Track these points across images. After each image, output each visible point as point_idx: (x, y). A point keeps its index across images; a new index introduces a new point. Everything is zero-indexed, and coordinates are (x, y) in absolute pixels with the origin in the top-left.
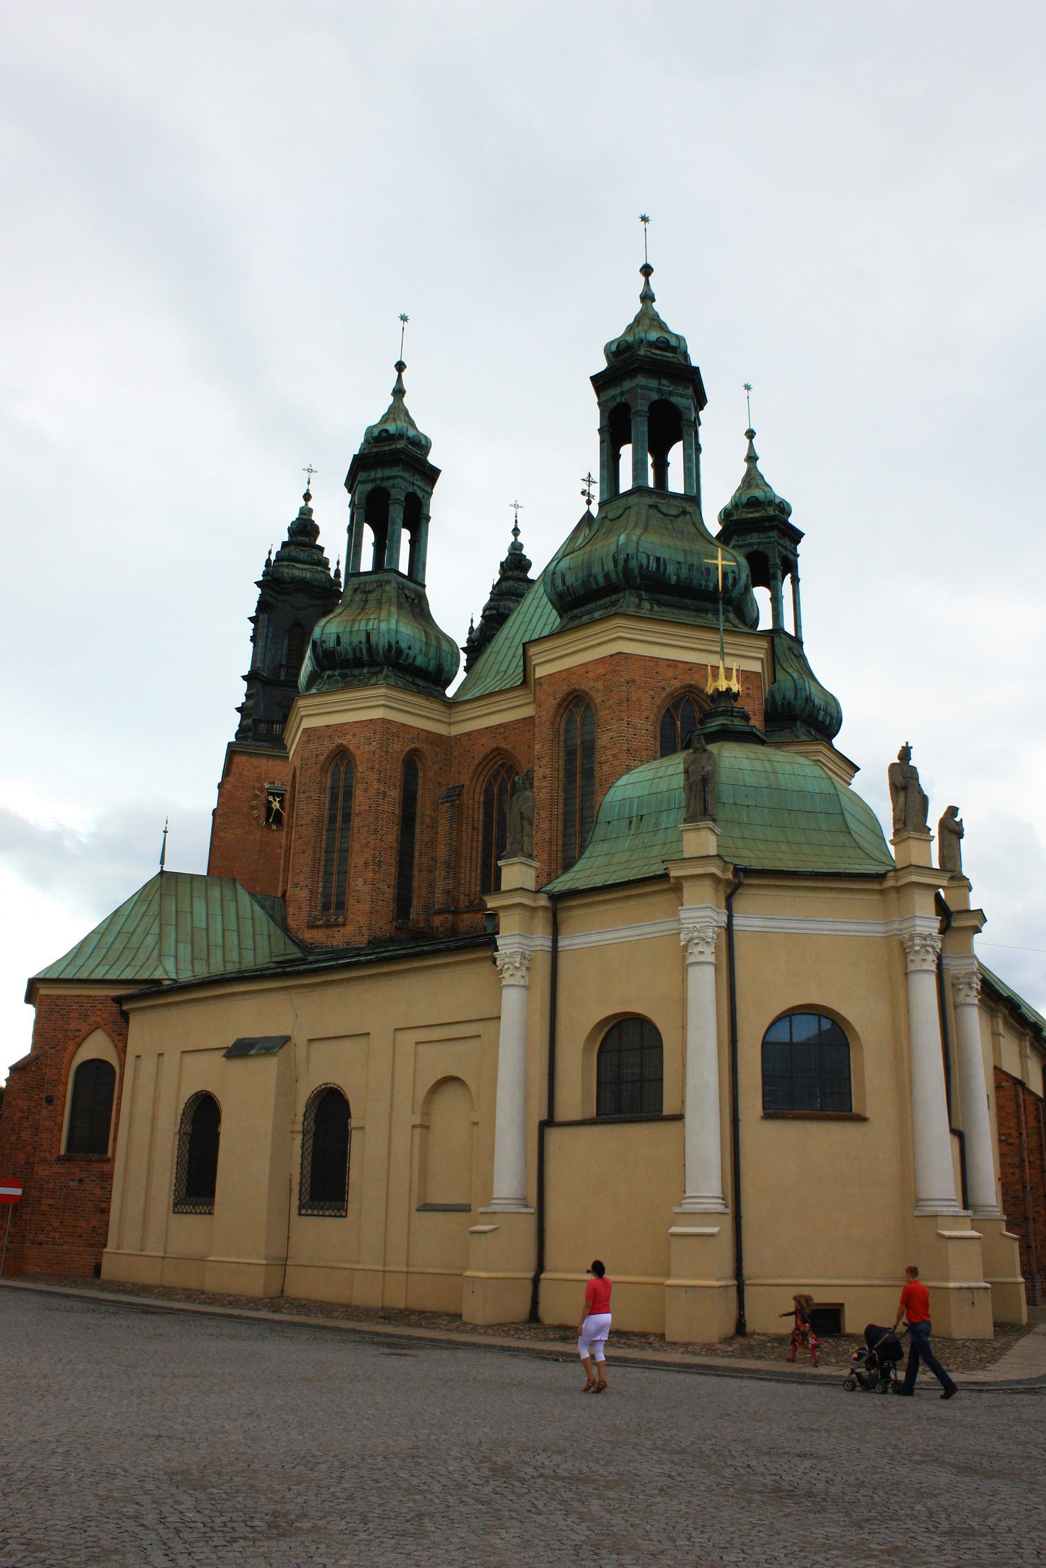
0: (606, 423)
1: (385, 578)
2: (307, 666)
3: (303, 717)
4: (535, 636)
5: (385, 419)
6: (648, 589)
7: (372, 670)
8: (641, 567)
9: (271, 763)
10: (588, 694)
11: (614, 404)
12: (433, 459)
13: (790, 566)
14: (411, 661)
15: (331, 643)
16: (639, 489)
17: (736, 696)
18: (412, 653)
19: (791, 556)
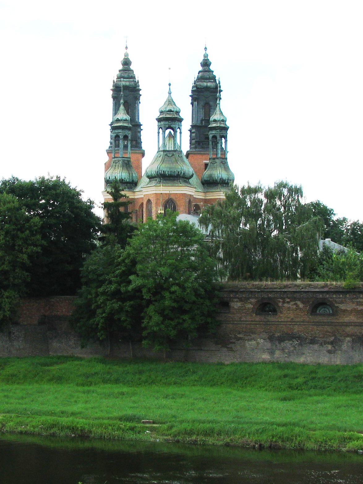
6: (162, 177)
15: (108, 178)
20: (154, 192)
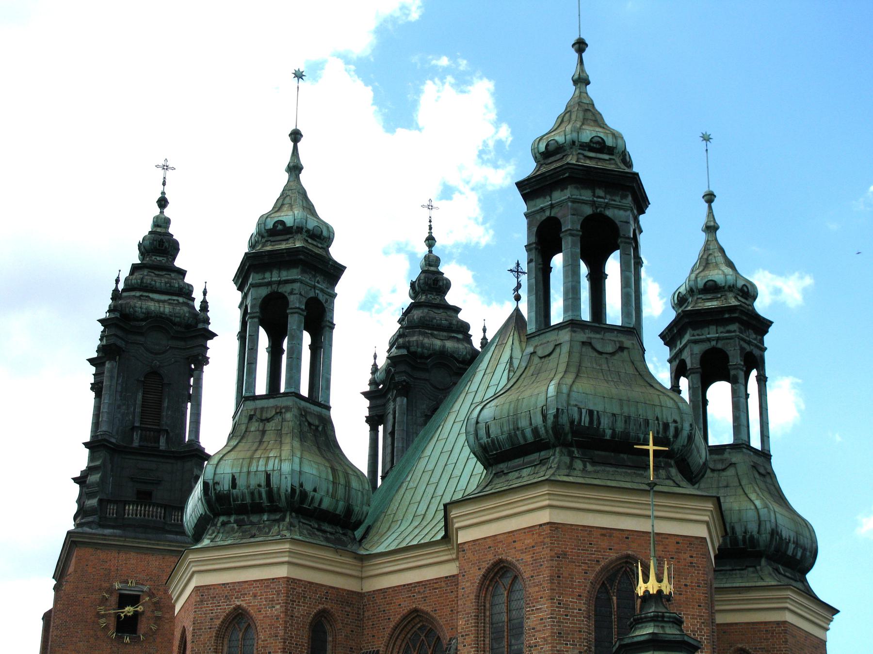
0: (533, 239)
1: (284, 404)
2: (194, 504)
3: (194, 573)
4: (458, 496)
5: (279, 206)
6: (579, 445)
7: (273, 517)
8: (572, 422)
9: (123, 556)
10: (515, 567)
11: (544, 218)
12: (337, 252)
13: (755, 360)
14: (316, 505)
15: (226, 485)
16: (573, 324)
17: (669, 598)
18: (318, 496)
19: (756, 352)
20: (544, 517)
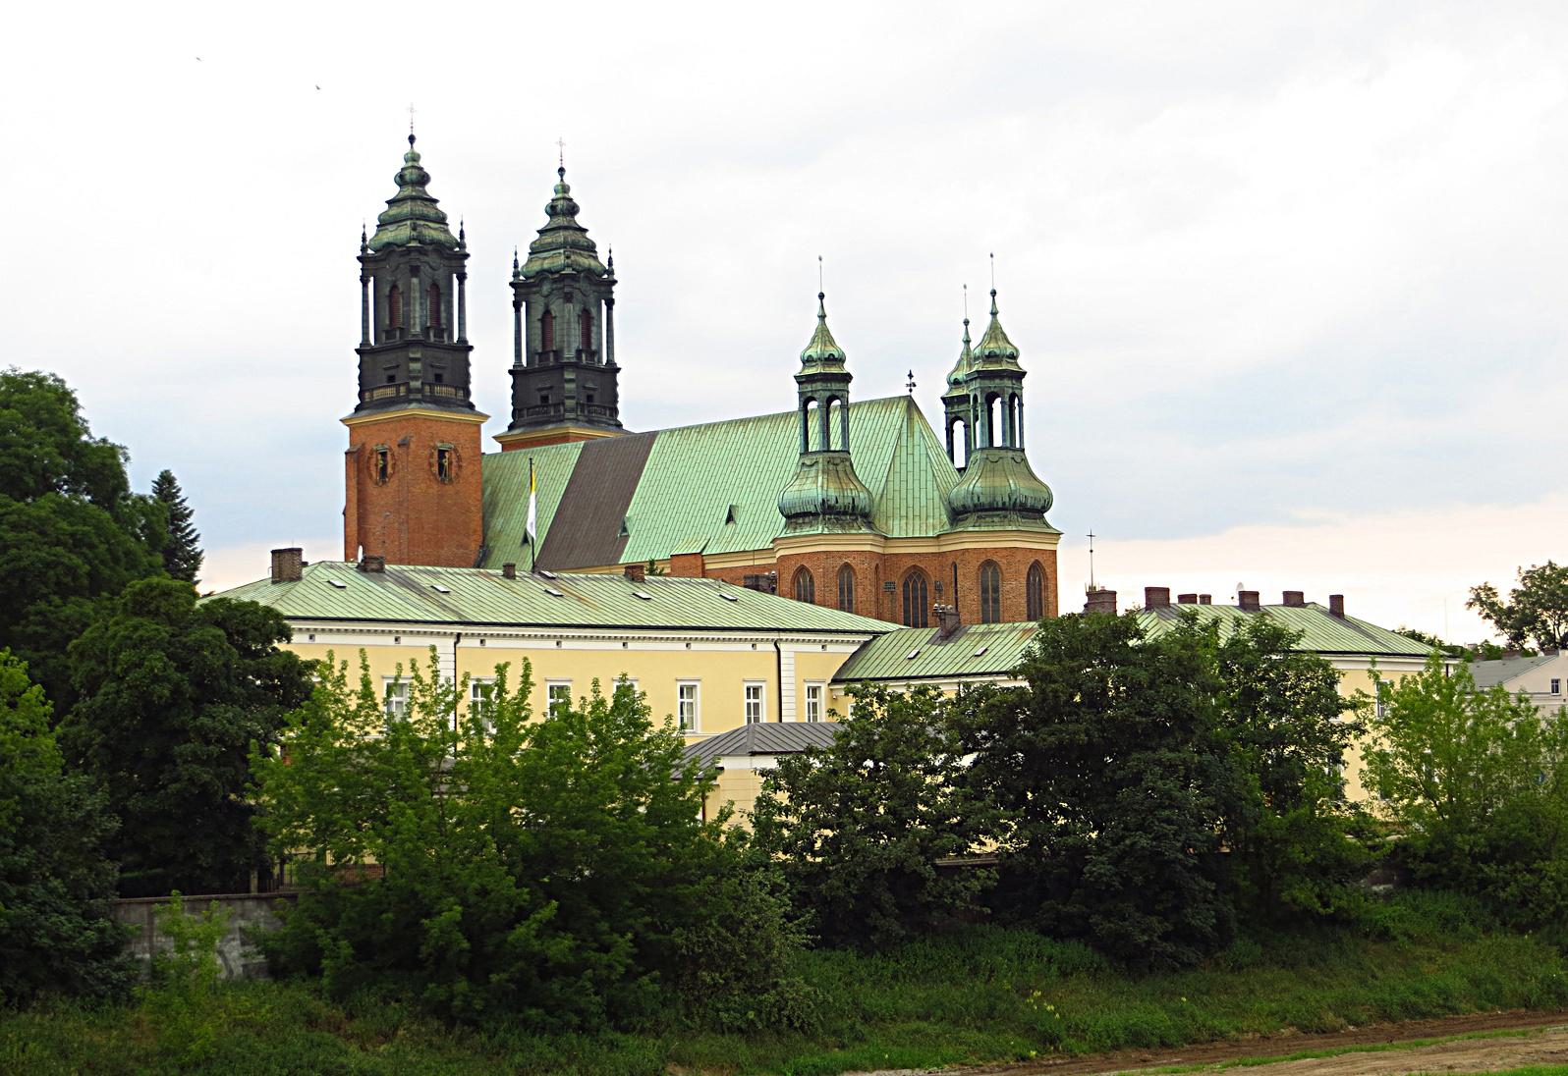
15: (833, 502)
